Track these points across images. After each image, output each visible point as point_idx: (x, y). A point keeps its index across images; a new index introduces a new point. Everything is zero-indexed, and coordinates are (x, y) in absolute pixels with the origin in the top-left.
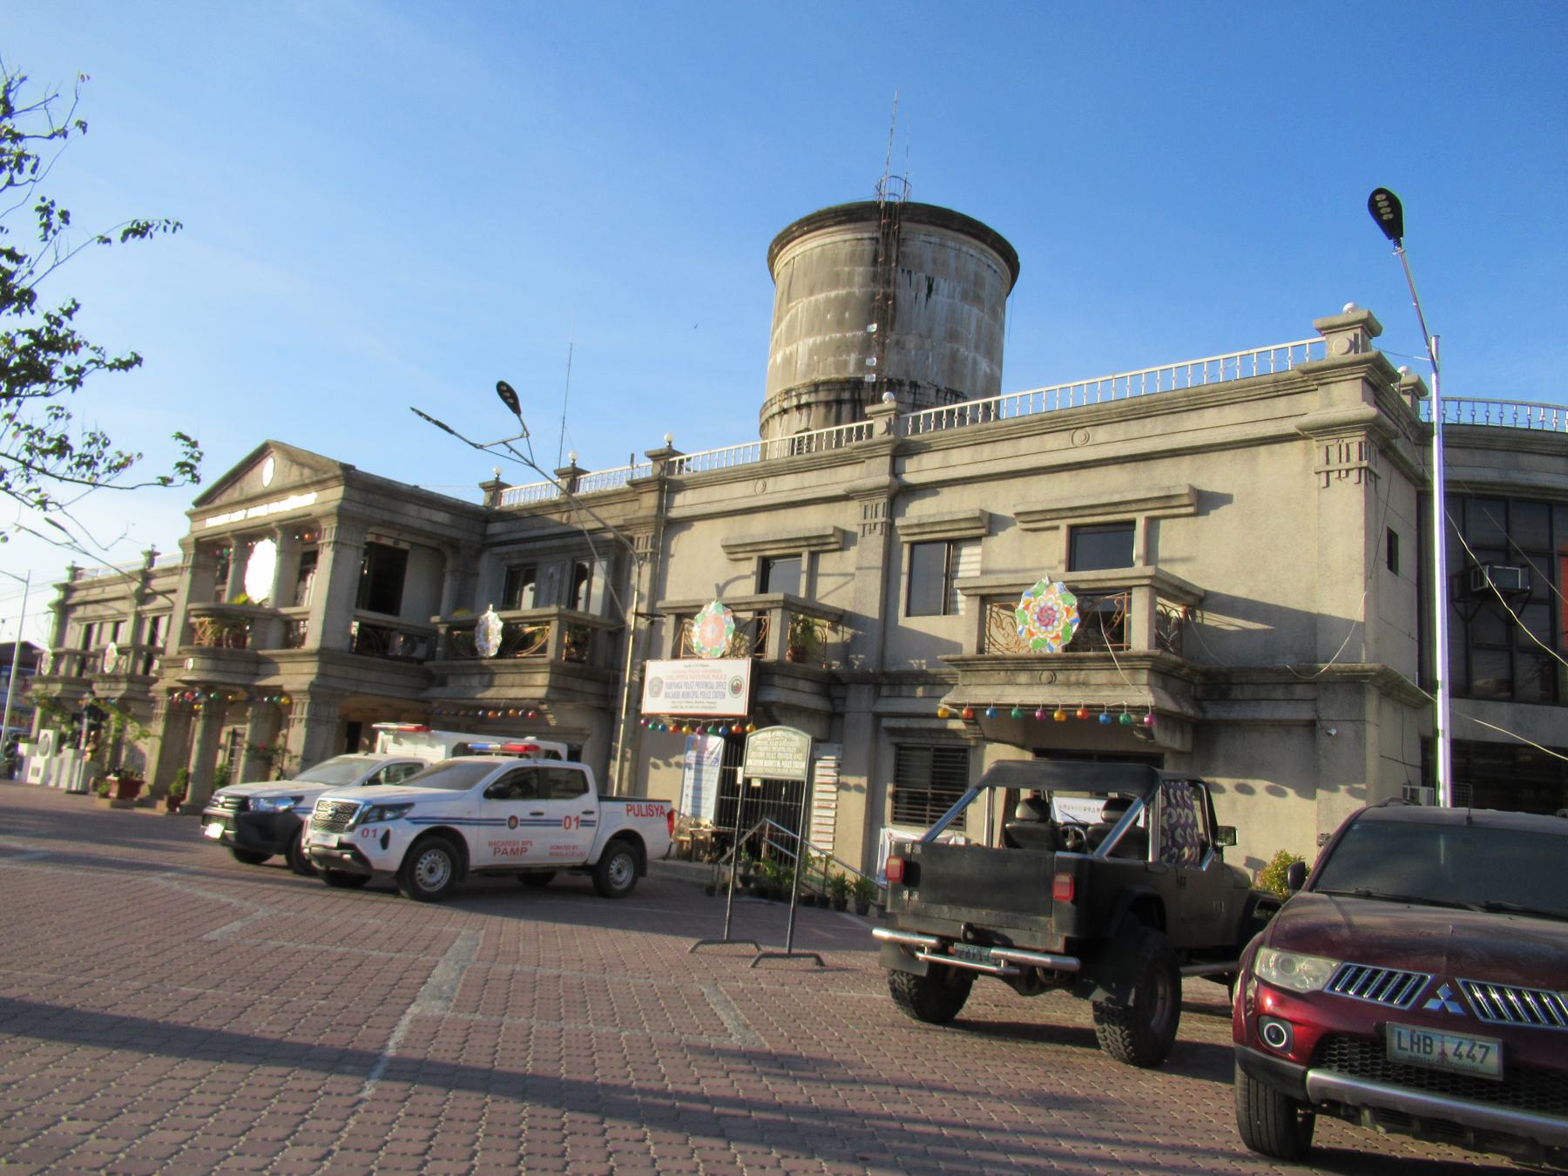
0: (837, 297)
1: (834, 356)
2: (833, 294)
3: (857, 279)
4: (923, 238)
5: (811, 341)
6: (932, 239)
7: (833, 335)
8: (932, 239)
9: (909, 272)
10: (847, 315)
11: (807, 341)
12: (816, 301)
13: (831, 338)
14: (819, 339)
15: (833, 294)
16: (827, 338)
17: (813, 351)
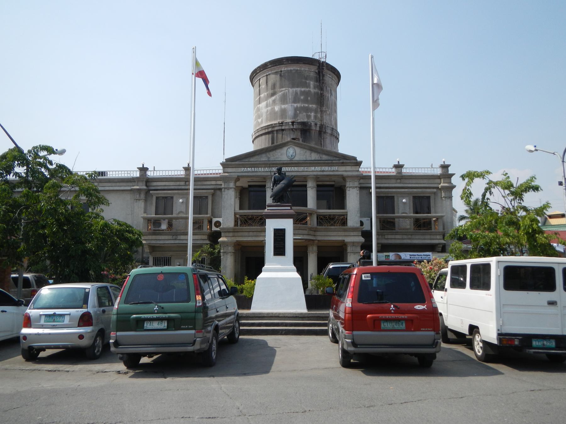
0: (304, 91)
1: (306, 113)
2: (303, 89)
3: (312, 86)
4: (328, 75)
5: (295, 105)
6: (330, 76)
7: (305, 105)
8: (330, 76)
9: (326, 87)
10: (309, 98)
11: (293, 104)
12: (296, 90)
13: (304, 106)
14: (299, 105)
15: (303, 89)
16: (302, 106)
17: (296, 109)
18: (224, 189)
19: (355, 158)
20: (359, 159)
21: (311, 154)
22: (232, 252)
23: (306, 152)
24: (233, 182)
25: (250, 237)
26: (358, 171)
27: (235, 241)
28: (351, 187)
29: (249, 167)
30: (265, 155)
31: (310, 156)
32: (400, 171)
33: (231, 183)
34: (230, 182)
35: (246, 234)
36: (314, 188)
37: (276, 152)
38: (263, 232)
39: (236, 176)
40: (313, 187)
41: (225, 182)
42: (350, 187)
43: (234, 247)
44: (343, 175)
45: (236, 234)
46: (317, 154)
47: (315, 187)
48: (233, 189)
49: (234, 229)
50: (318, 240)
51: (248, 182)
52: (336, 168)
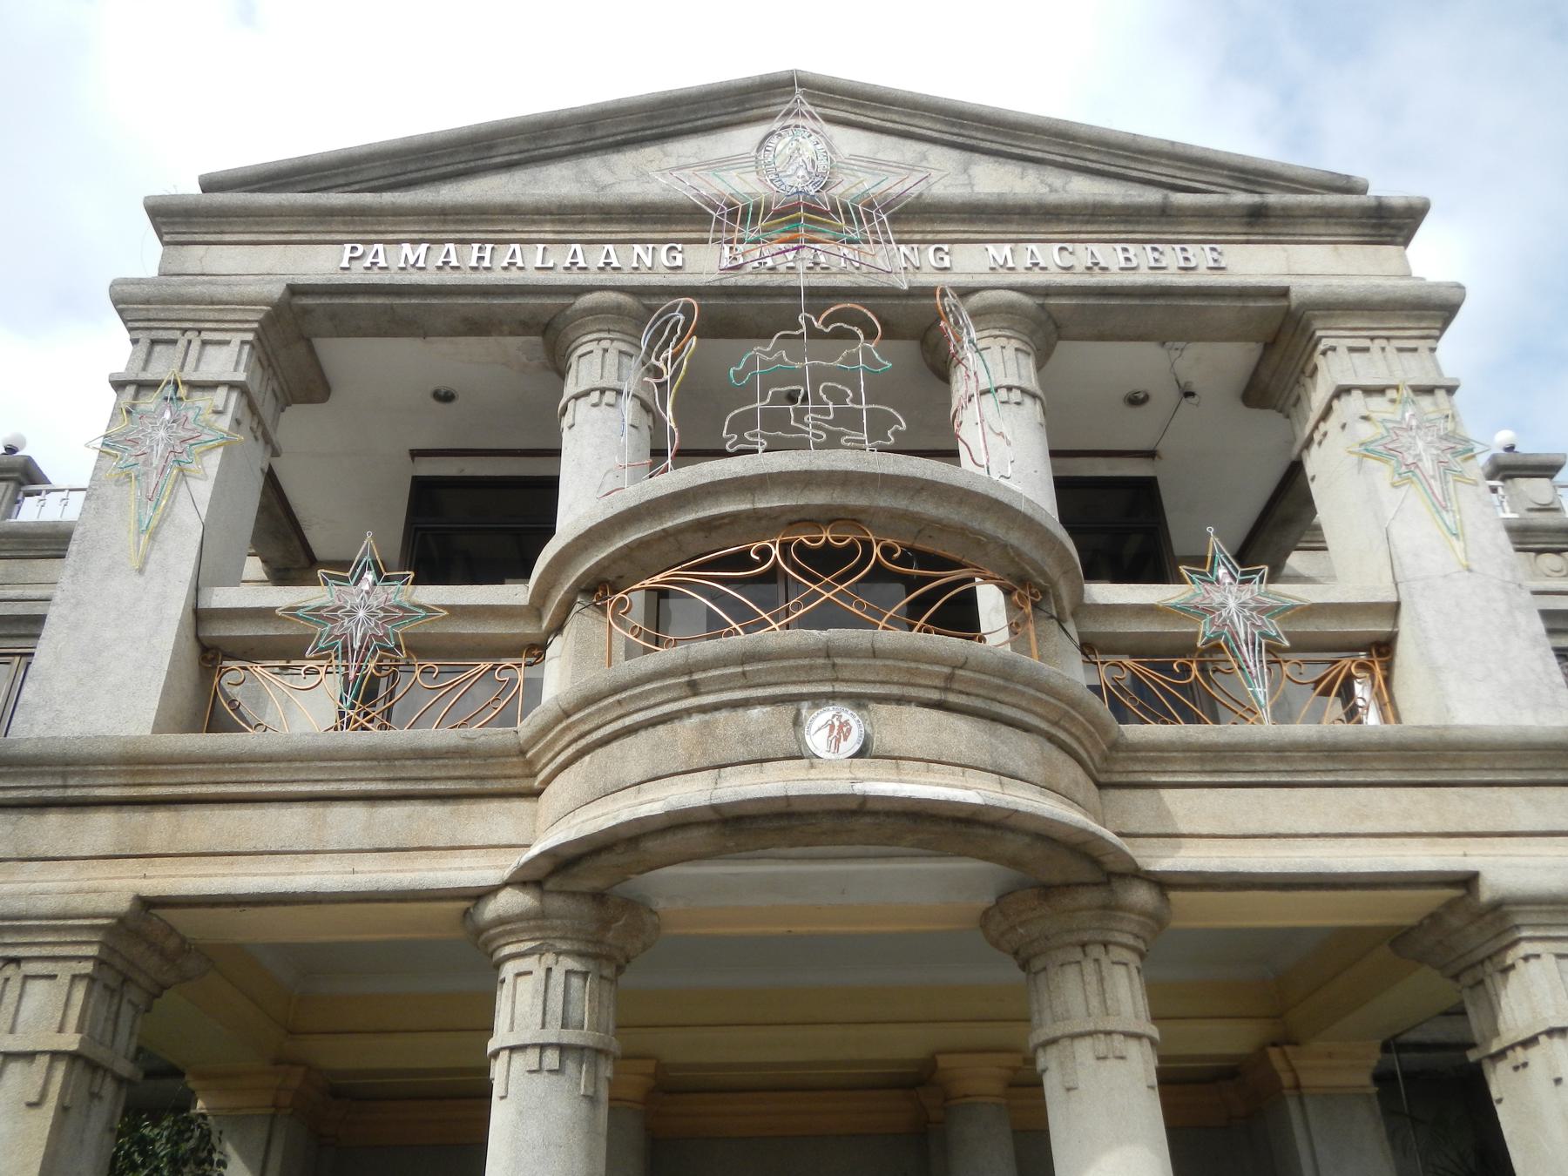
18: (131, 390)
19: (1348, 186)
20: (1387, 187)
21: (965, 170)
22: (55, 1055)
23: (924, 157)
24: (236, 338)
25: (321, 863)
26: (1408, 276)
27: (123, 905)
28: (1381, 391)
29: (413, 242)
30: (565, 172)
31: (963, 178)
32: (1545, 498)
33: (211, 351)
34: (205, 343)
35: (289, 823)
36: (1028, 401)
37: (666, 155)
38: (495, 806)
39: (276, 290)
40: (1024, 391)
41: (154, 342)
42: (1369, 391)
43: (91, 979)
44: (1284, 292)
45: (160, 827)
46: (1020, 170)
47: (1034, 396)
48: (222, 392)
49: (135, 763)
50: (1164, 883)
51: (416, 454)
52: (1201, 255)
